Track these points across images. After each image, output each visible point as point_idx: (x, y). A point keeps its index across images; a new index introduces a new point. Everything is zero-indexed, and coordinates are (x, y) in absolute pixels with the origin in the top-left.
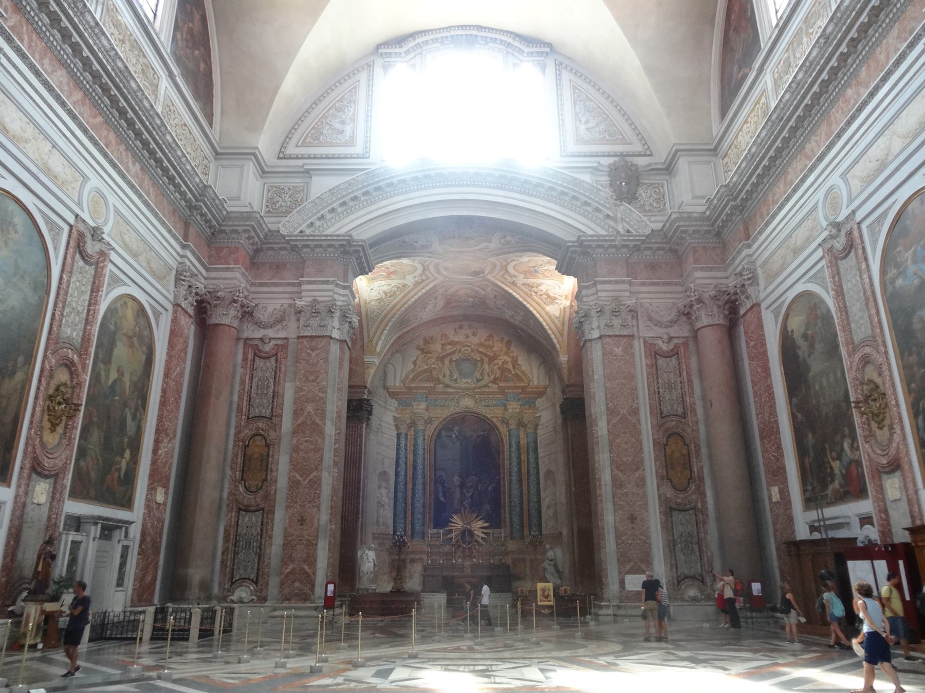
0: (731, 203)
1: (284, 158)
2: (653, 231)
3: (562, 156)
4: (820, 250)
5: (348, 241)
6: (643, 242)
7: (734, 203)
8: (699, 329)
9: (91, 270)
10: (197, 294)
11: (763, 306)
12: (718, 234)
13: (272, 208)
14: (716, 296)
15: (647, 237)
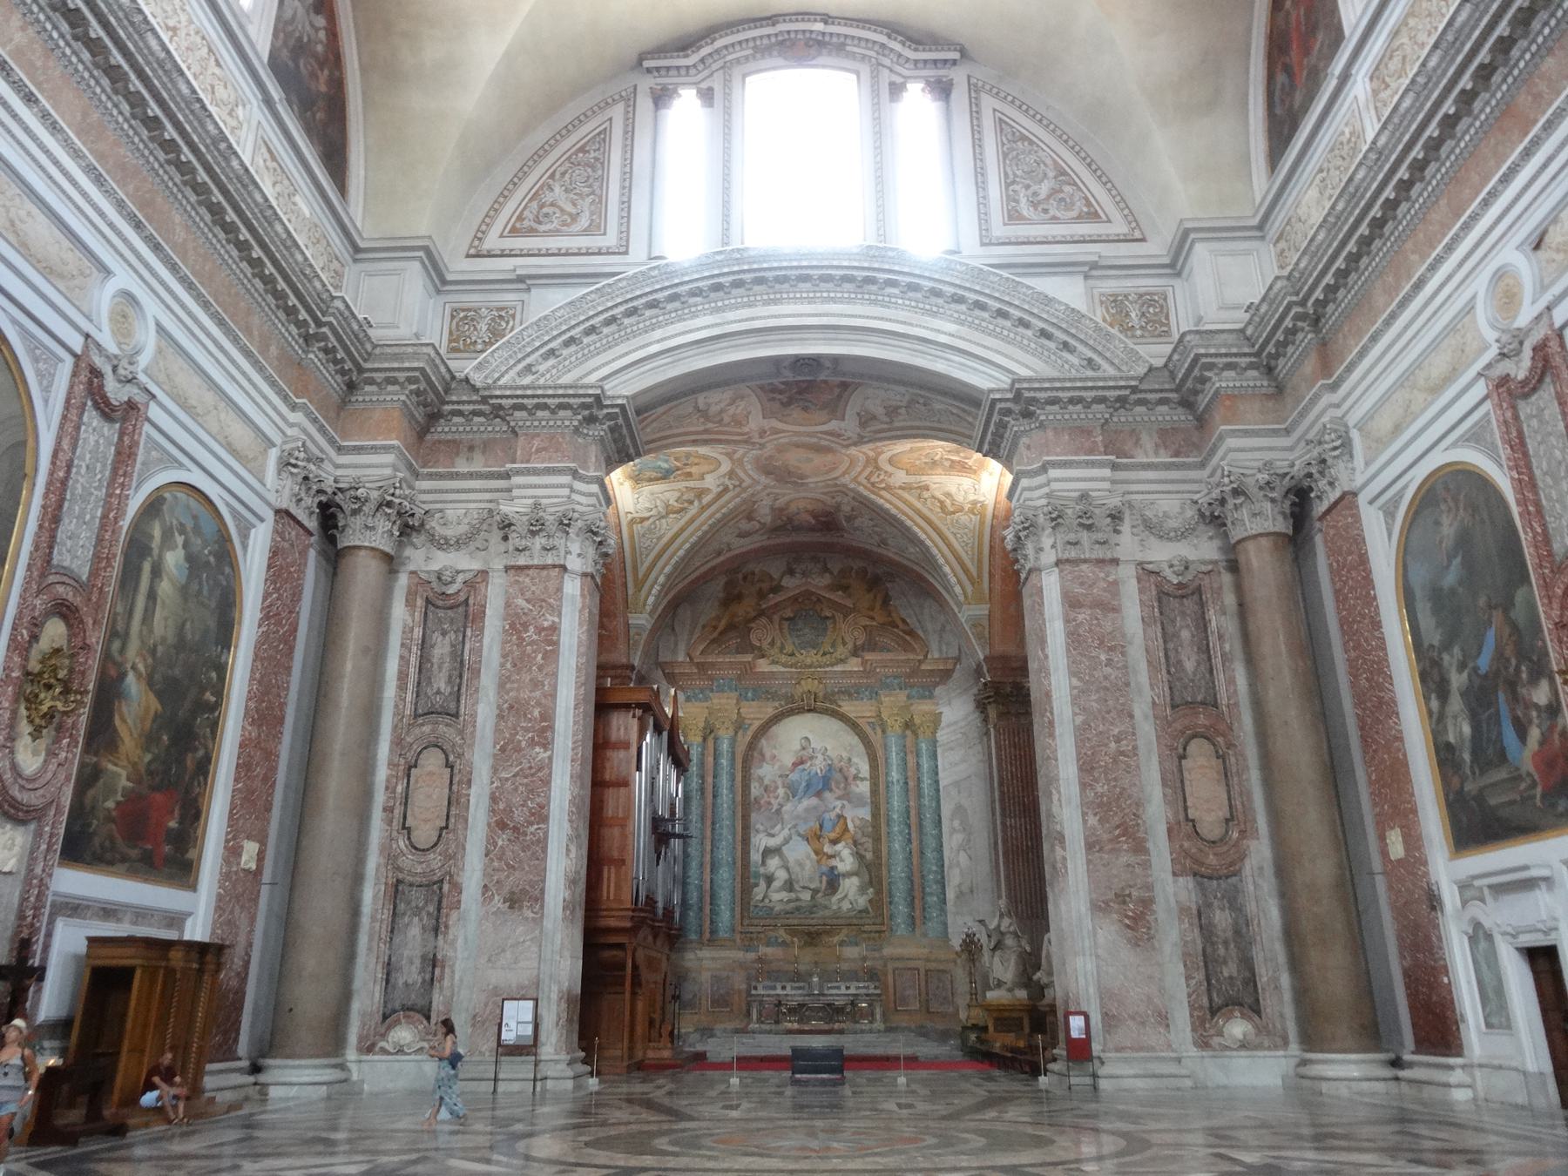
0: (1296, 310)
1: (478, 256)
2: (1151, 369)
3: (983, 244)
4: (1482, 382)
5: (598, 398)
6: (1134, 389)
7: (1300, 309)
8: (1239, 542)
9: (110, 431)
10: (320, 491)
11: (1362, 500)
12: (1270, 370)
13: (461, 343)
14: (1268, 483)
15: (1141, 380)
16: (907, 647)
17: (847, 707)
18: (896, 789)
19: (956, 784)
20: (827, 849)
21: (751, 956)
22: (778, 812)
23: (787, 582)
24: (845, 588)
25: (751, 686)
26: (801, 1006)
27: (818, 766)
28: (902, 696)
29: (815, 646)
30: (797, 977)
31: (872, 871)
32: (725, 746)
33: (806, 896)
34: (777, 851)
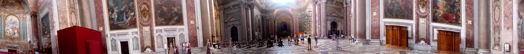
16: (23, 10)
17: (16, 15)
18: (22, 24)
19: (29, 25)
20: (14, 30)
21: (5, 41)
22: (9, 25)
23: (10, 1)
24: (16, 2)
25: (6, 12)
26: (11, 47)
27: (13, 21)
28: (22, 15)
29: (13, 8)
30: (10, 43)
31: (19, 33)
32: (3, 18)
33: (12, 35)
34: (8, 30)
